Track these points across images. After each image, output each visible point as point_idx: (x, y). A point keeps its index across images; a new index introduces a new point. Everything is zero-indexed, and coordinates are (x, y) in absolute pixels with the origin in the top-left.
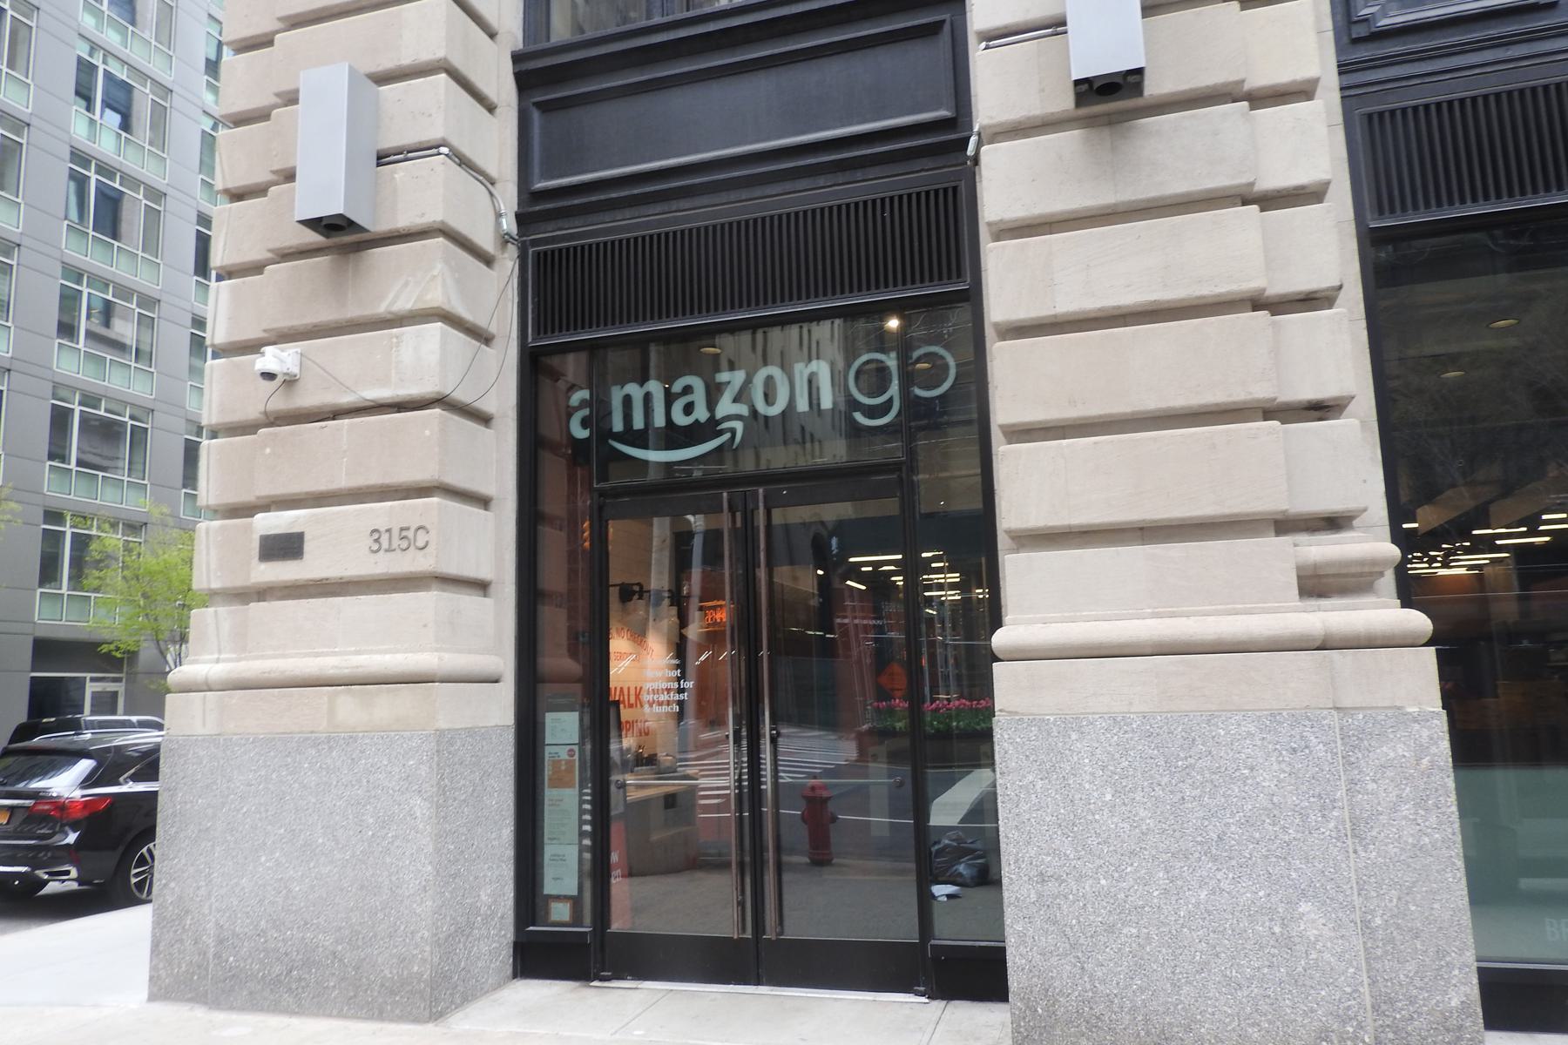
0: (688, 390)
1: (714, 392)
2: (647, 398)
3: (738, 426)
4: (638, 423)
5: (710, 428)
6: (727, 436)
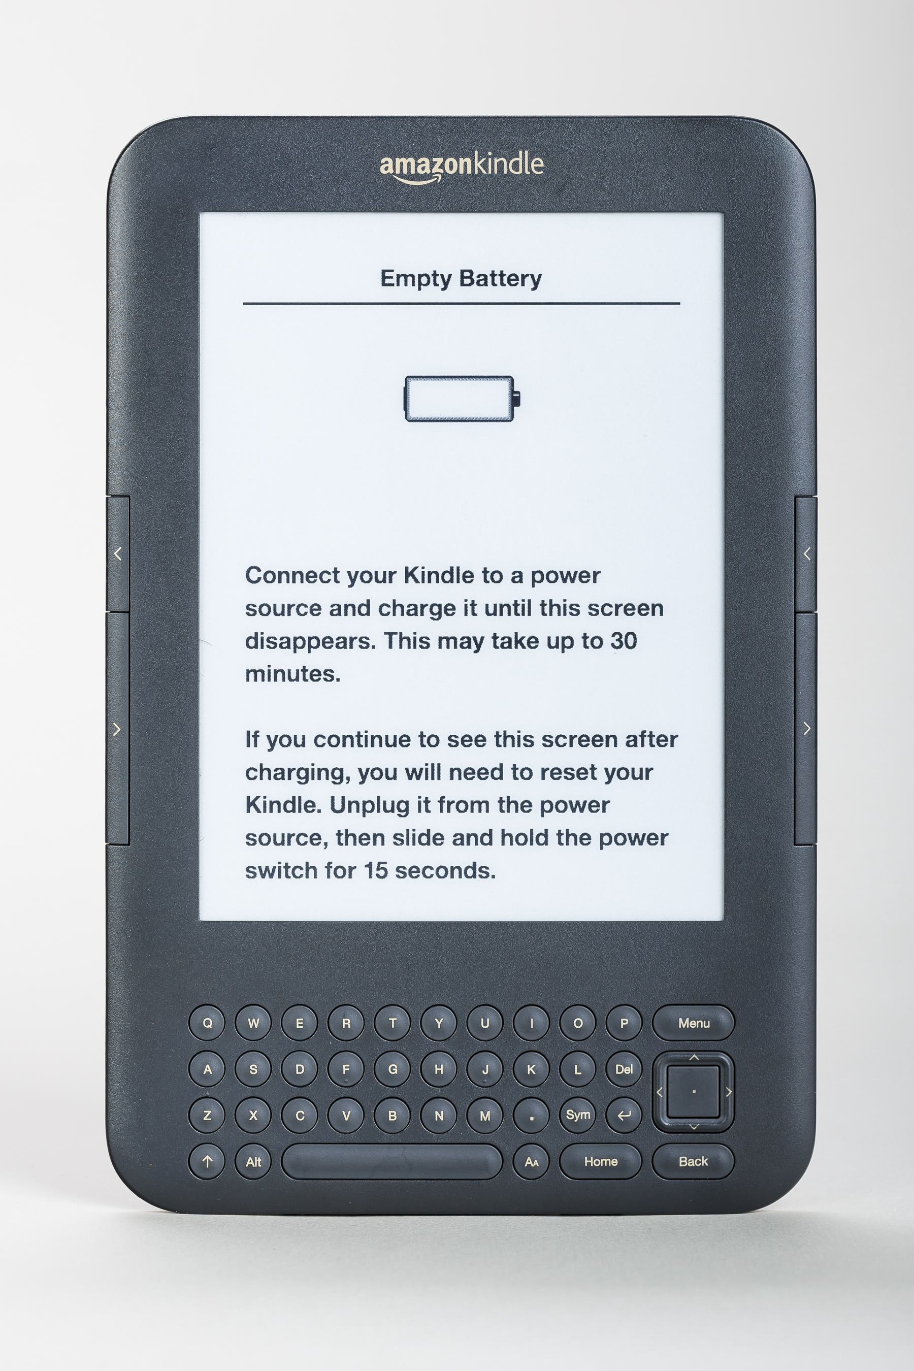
0: (423, 162)
1: (432, 164)
2: (409, 164)
3: (440, 176)
4: (405, 172)
5: (429, 176)
6: (436, 179)
